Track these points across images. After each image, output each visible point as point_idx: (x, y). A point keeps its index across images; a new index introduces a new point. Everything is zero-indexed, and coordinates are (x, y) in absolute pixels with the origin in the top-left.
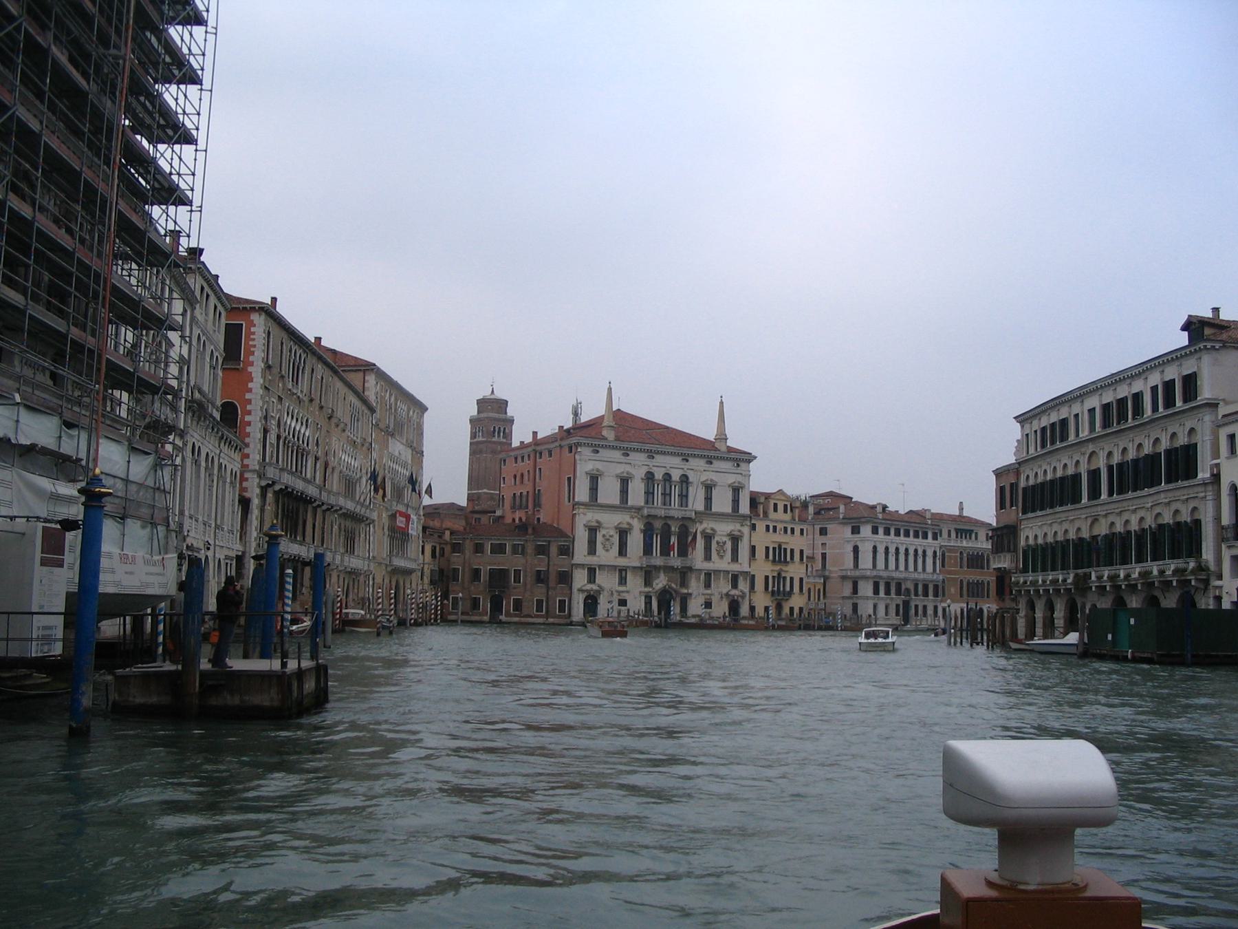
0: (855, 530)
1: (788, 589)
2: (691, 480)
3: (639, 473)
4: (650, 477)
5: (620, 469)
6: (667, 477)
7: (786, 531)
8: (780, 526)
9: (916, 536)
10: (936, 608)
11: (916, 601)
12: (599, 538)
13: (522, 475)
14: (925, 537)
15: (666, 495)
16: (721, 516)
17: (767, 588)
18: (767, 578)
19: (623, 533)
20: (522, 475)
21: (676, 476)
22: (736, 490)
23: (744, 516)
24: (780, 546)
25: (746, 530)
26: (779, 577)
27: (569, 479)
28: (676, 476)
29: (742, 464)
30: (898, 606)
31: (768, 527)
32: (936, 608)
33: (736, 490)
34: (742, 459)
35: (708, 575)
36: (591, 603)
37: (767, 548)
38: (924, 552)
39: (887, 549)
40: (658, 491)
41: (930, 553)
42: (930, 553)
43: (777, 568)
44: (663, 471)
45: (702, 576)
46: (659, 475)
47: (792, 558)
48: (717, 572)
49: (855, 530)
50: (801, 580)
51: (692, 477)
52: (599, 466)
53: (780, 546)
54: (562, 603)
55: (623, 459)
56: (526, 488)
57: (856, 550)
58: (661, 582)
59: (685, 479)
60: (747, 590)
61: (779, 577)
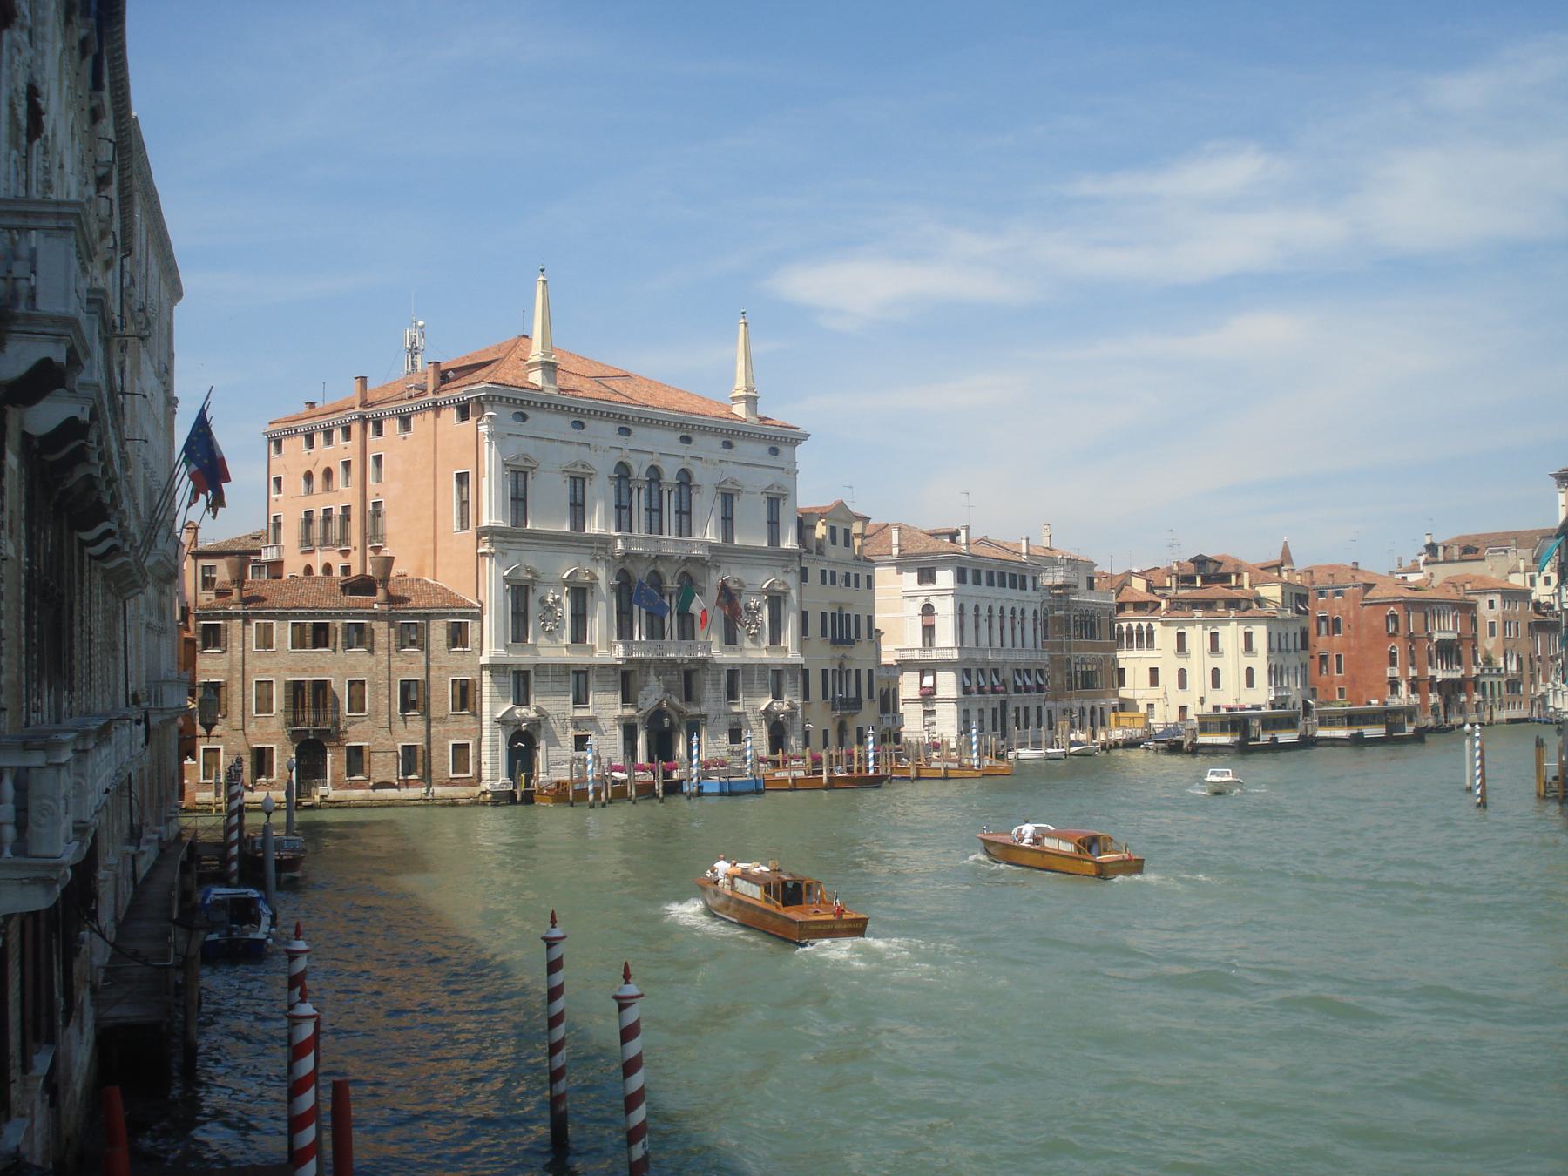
0: (926, 576)
1: (853, 694)
2: (696, 479)
3: (604, 466)
4: (623, 473)
5: (570, 455)
6: (655, 473)
7: (848, 584)
8: (840, 572)
9: (1013, 586)
10: (1039, 709)
11: (1016, 701)
12: (534, 607)
13: (328, 473)
14: (1024, 587)
15: (654, 511)
16: (750, 555)
17: (825, 696)
18: (825, 672)
19: (581, 594)
20: (328, 473)
21: (669, 475)
22: (774, 503)
23: (789, 553)
24: (840, 609)
25: (792, 580)
26: (841, 672)
27: (462, 478)
28: (669, 475)
29: (783, 449)
30: (994, 710)
31: (823, 572)
32: (1039, 709)
33: (774, 503)
34: (781, 441)
35: (732, 674)
36: (522, 745)
37: (824, 615)
38: (1023, 611)
39: (977, 608)
40: (639, 502)
41: (1029, 615)
42: (1029, 615)
43: (840, 651)
44: (648, 461)
45: (724, 678)
46: (639, 472)
47: (858, 635)
48: (748, 668)
49: (926, 576)
50: (870, 671)
51: (699, 474)
52: (529, 447)
53: (840, 609)
54: (460, 749)
55: (574, 435)
56: (344, 494)
57: (928, 610)
58: (652, 694)
59: (685, 480)
60: (798, 701)
61: (841, 672)
